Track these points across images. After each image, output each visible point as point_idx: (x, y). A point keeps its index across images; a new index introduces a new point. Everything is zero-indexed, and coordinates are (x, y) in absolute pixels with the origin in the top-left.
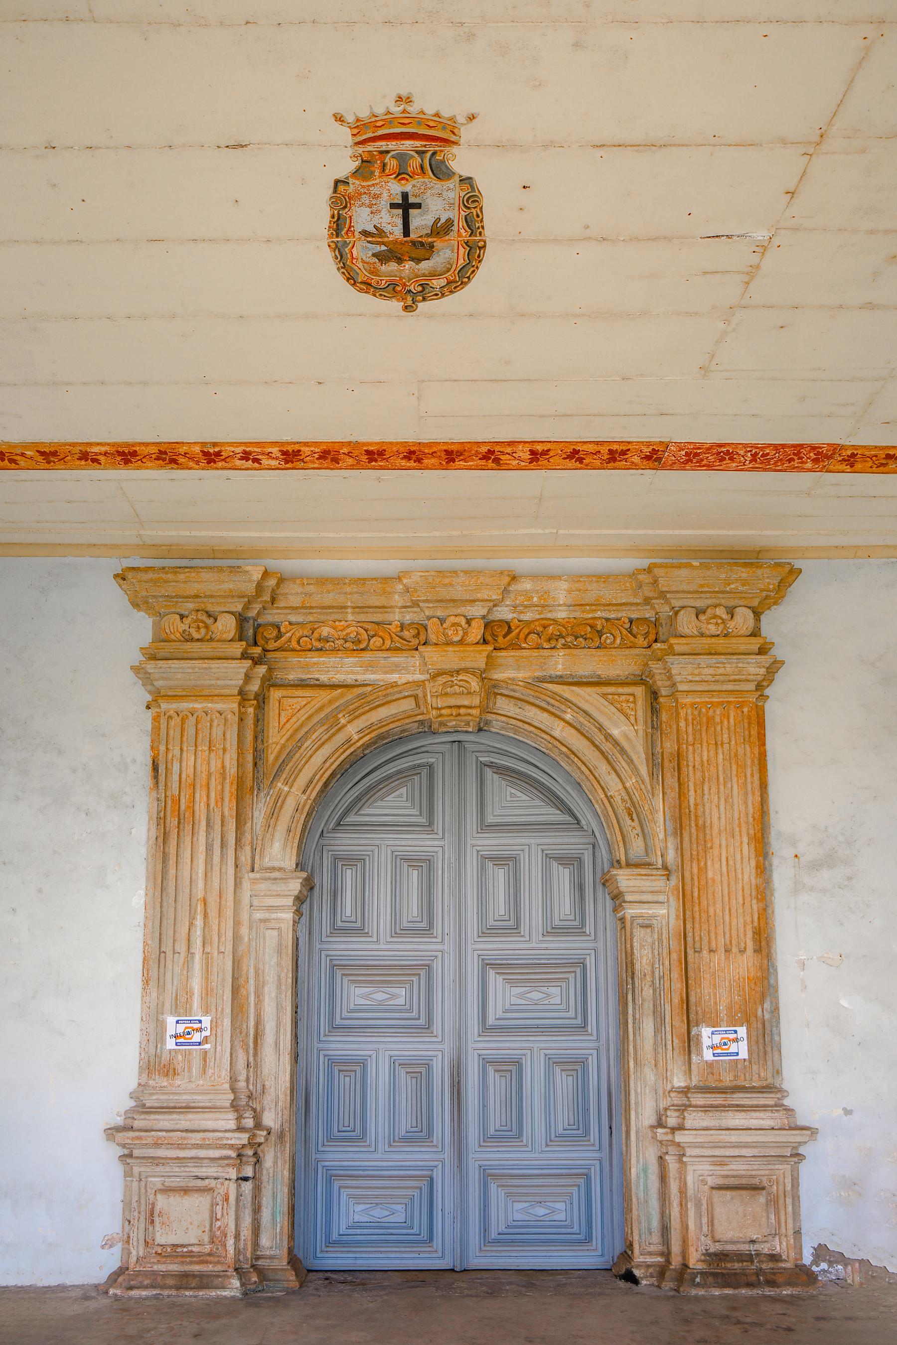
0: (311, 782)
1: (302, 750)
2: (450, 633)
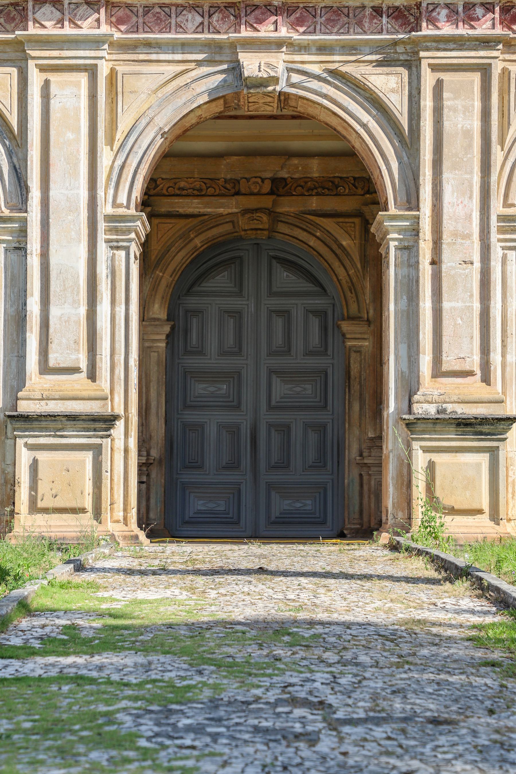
0: (175, 270)
1: (170, 253)
2: (252, 187)
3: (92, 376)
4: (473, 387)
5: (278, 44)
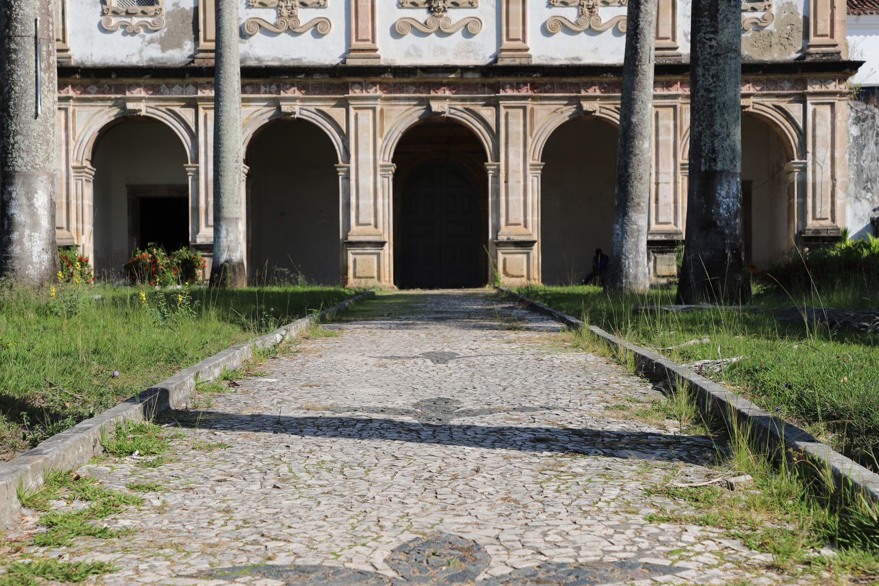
3: (376, 226)
4: (521, 229)
5: (445, 98)
